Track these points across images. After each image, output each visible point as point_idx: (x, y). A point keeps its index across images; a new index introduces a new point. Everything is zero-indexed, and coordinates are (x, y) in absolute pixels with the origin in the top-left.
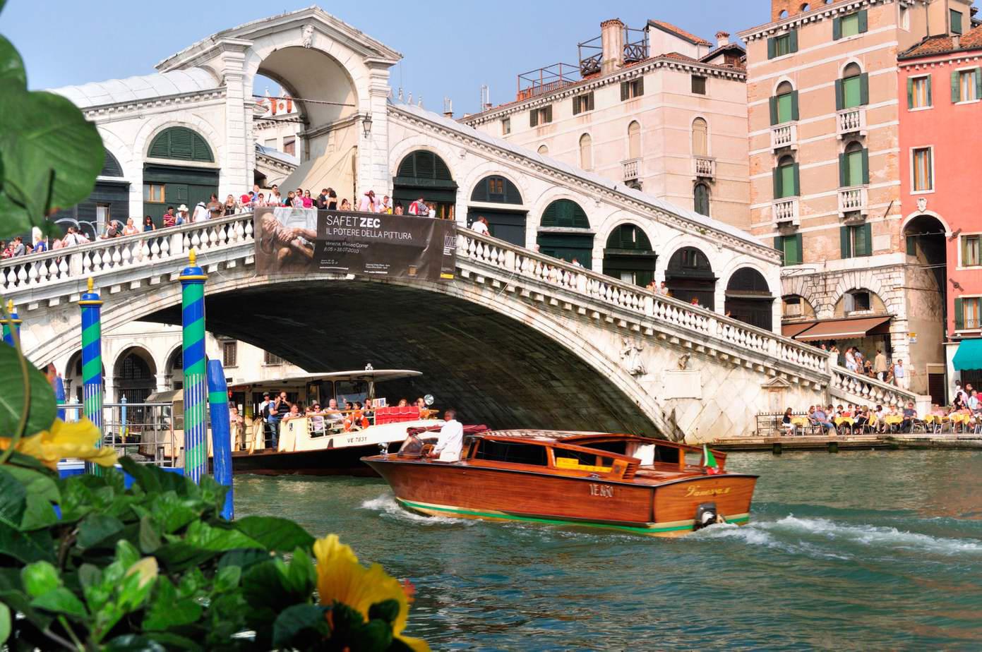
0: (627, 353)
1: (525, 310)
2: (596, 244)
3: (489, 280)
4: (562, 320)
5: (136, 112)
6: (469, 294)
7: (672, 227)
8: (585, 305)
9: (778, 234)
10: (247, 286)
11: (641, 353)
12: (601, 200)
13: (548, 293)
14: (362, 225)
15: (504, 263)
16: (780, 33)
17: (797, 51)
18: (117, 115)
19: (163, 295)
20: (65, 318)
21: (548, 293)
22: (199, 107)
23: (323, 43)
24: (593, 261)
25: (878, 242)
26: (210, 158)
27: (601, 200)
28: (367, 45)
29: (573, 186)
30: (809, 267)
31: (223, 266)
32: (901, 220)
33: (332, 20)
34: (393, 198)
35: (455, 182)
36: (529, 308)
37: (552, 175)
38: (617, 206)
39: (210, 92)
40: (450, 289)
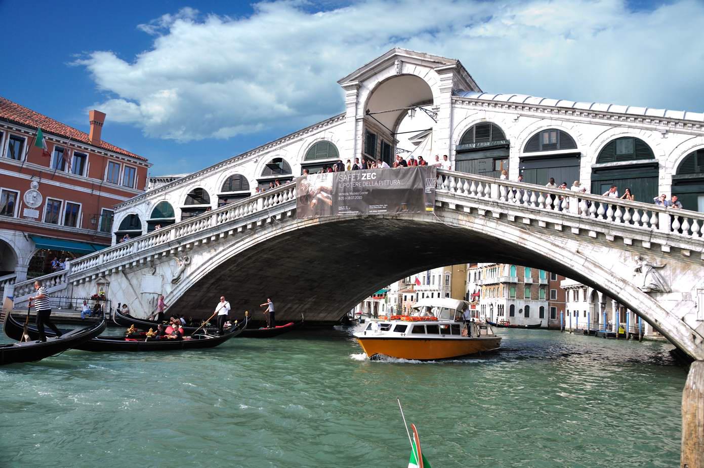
0: (638, 270)
2: (660, 171)
3: (472, 209)
4: (559, 241)
5: (299, 138)
6: (464, 223)
8: (577, 225)
10: (304, 226)
11: (662, 272)
12: (667, 131)
14: (363, 179)
15: (490, 194)
18: (291, 141)
20: (215, 250)
21: (533, 217)
22: (332, 127)
23: (408, 69)
24: (659, 187)
26: (337, 155)
27: (667, 131)
28: (432, 60)
33: (407, 52)
34: (456, 161)
35: (507, 141)
36: (520, 231)
37: (608, 119)
38: (691, 134)
40: (446, 219)
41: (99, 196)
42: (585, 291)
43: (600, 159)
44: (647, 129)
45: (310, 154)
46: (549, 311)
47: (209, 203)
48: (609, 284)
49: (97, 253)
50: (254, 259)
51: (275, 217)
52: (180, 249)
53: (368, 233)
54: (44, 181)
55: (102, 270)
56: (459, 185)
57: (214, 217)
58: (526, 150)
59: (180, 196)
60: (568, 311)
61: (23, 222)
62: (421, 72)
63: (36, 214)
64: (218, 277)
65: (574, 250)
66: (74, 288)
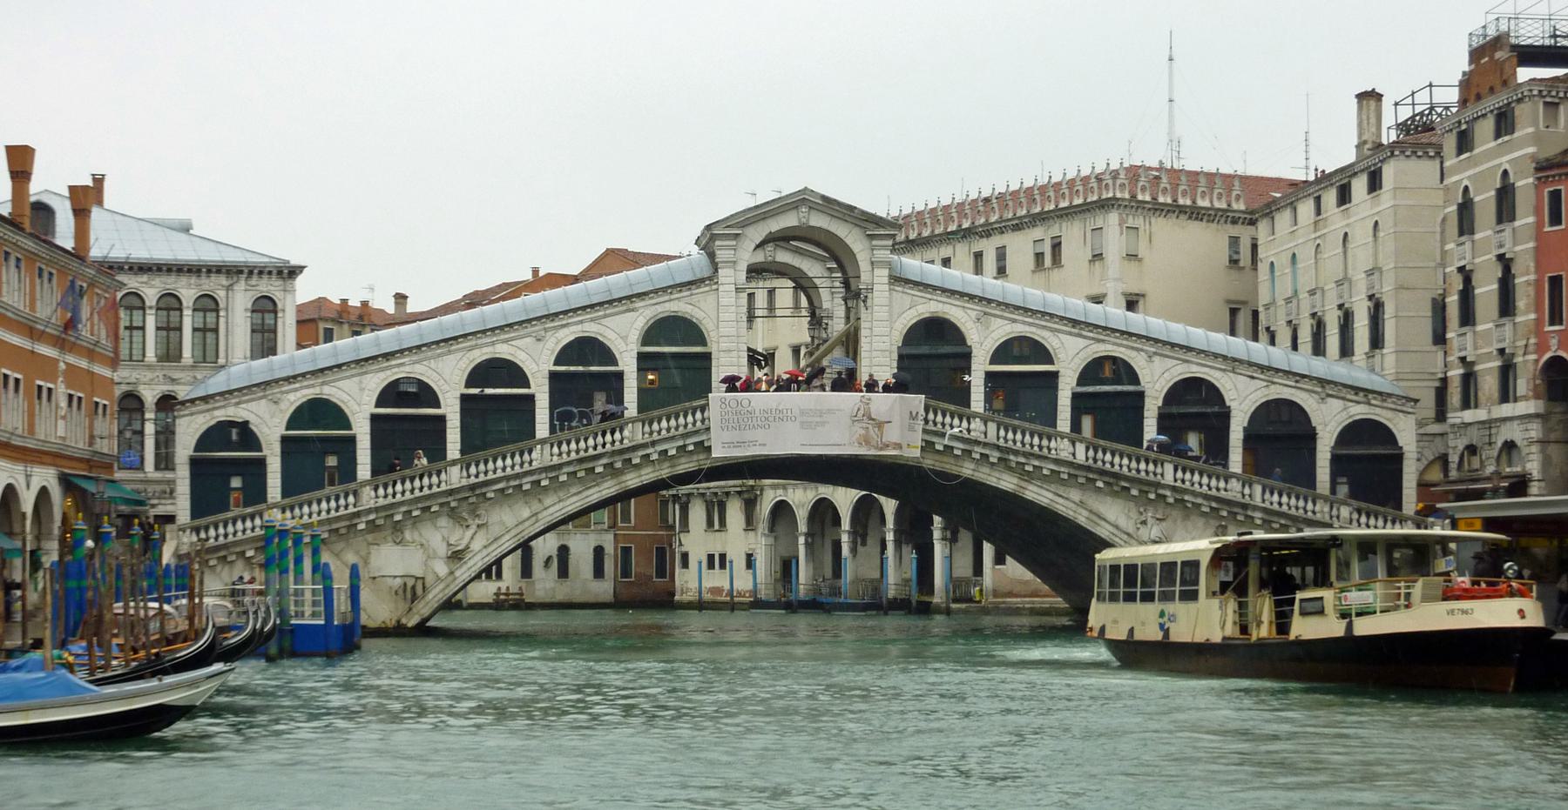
1: (1015, 481)
2: (1147, 401)
9: (1461, 371)
13: (1036, 463)
16: (1464, 127)
17: (1471, 150)
19: (629, 476)
21: (1036, 463)
23: (818, 221)
25: (1522, 386)
26: (702, 341)
30: (1480, 414)
31: (682, 449)
32: (1537, 361)
33: (824, 198)
39: (702, 281)
42: (750, 505)
43: (1081, 382)
44: (1133, 348)
46: (616, 556)
47: (439, 406)
52: (472, 500)
56: (948, 420)
59: (362, 390)
60: (685, 556)
62: (841, 230)
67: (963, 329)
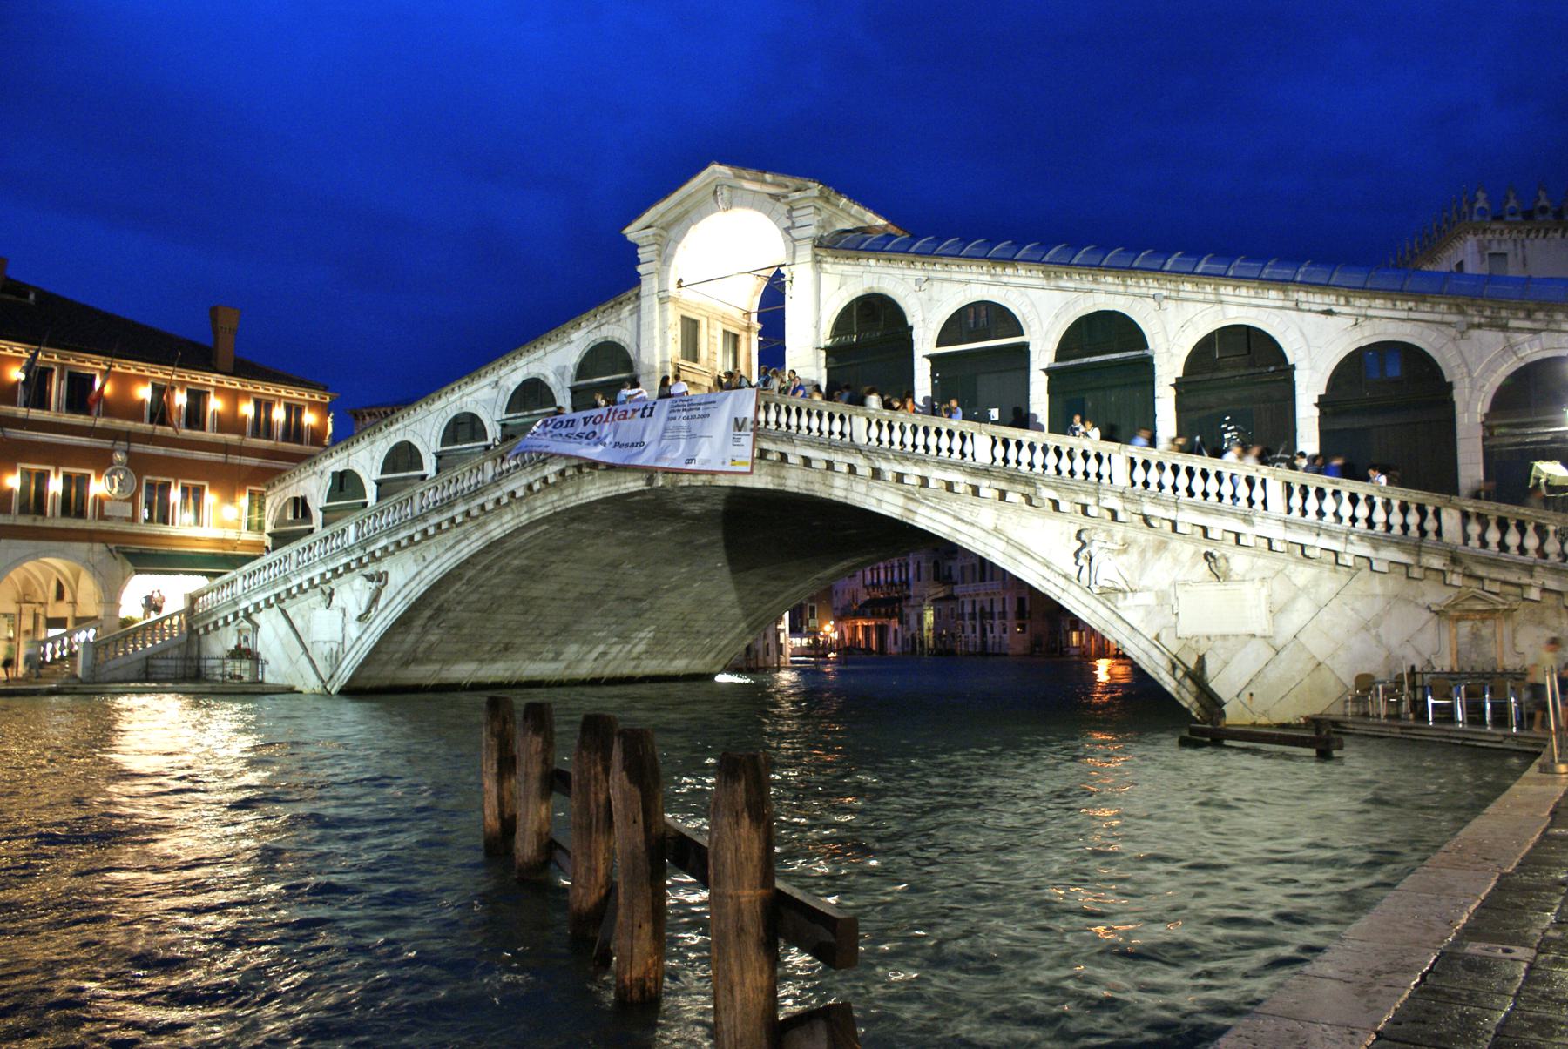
1: (901, 501)
7: (1329, 312)
19: (492, 526)
29: (1112, 288)
41: (239, 465)
45: (583, 369)
48: (1044, 583)
49: (233, 573)
50: (496, 568)
51: (513, 494)
53: (695, 508)
54: (137, 448)
55: (243, 605)
57: (417, 500)
58: (939, 344)
61: (105, 526)
63: (127, 510)
64: (436, 605)
65: (992, 526)
66: (203, 639)
67: (902, 305)
